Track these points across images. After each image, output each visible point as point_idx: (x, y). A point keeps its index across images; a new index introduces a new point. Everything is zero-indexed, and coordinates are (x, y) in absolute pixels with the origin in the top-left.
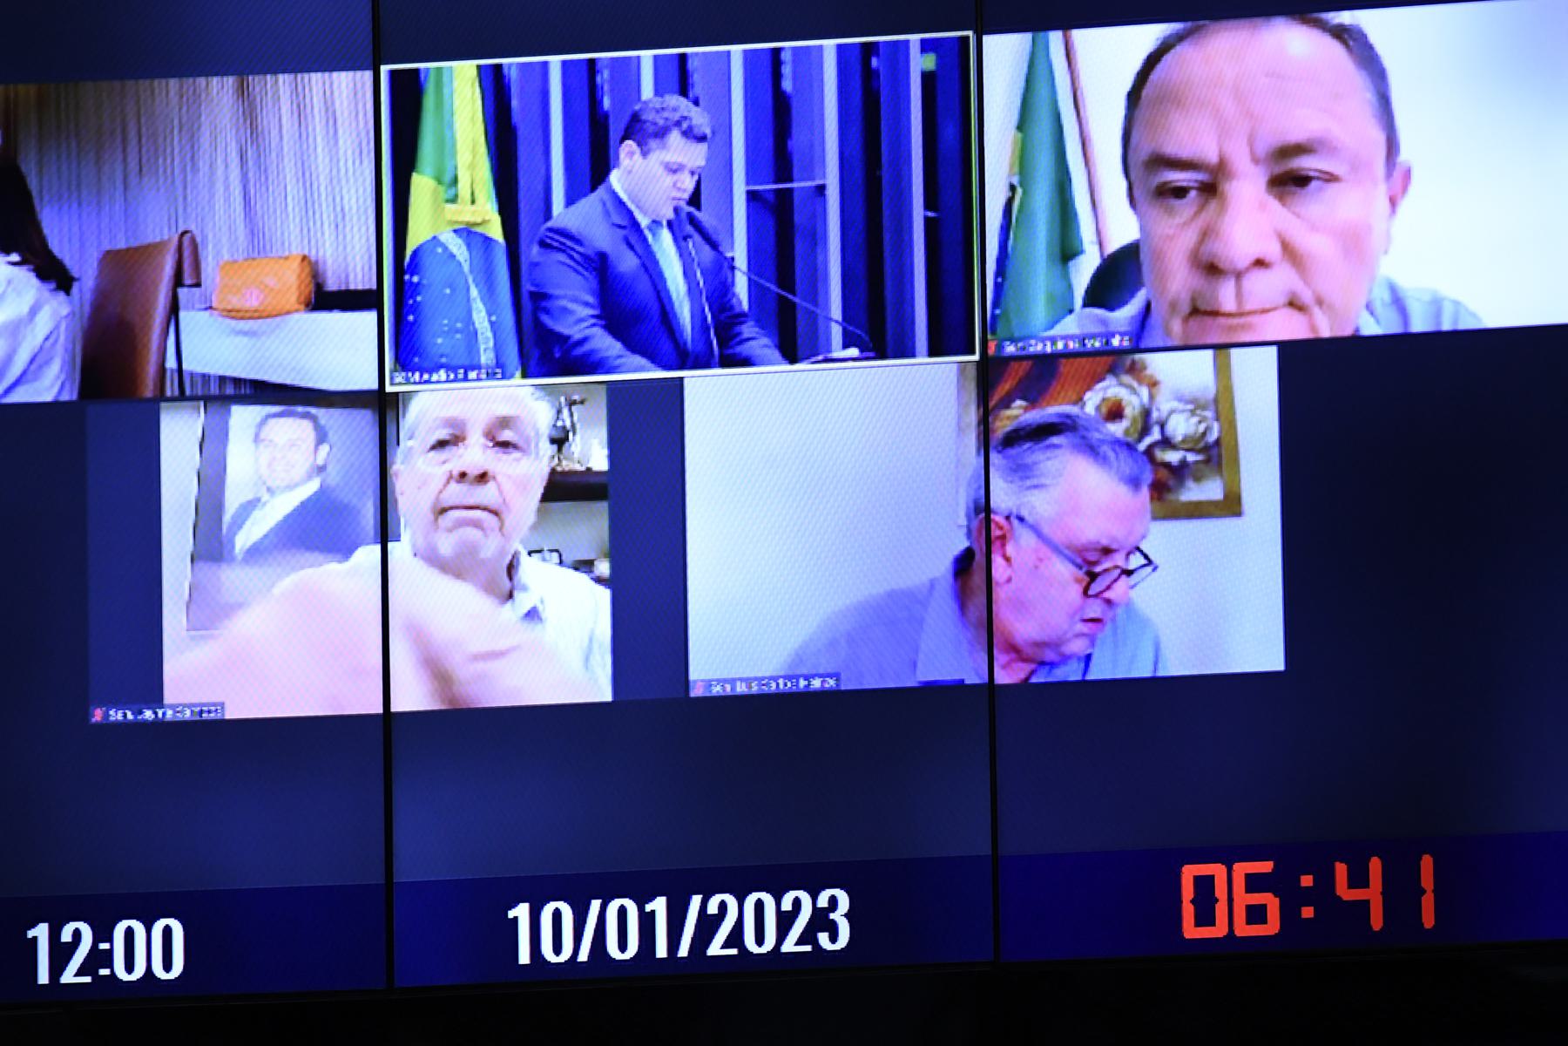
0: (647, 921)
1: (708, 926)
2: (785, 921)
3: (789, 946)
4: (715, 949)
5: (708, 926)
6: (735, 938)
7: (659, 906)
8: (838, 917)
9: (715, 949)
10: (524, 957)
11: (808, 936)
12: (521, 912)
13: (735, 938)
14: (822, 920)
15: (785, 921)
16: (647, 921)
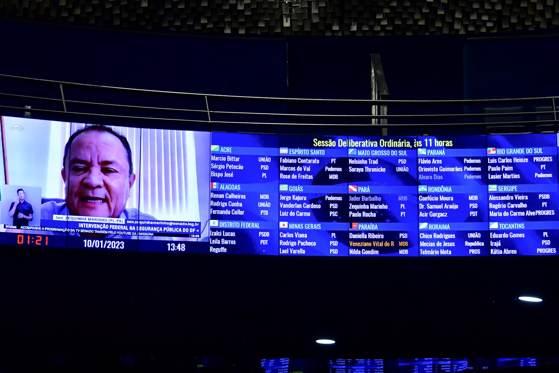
0: (100, 243)
1: (107, 244)
2: (116, 245)
3: (117, 248)
4: (108, 247)
5: (107, 244)
6: (111, 246)
7: (102, 242)
8: (123, 245)
9: (108, 247)
10: (85, 246)
11: (119, 247)
12: (85, 241)
13: (111, 246)
14: (121, 245)
15: (116, 245)
16: (100, 243)
